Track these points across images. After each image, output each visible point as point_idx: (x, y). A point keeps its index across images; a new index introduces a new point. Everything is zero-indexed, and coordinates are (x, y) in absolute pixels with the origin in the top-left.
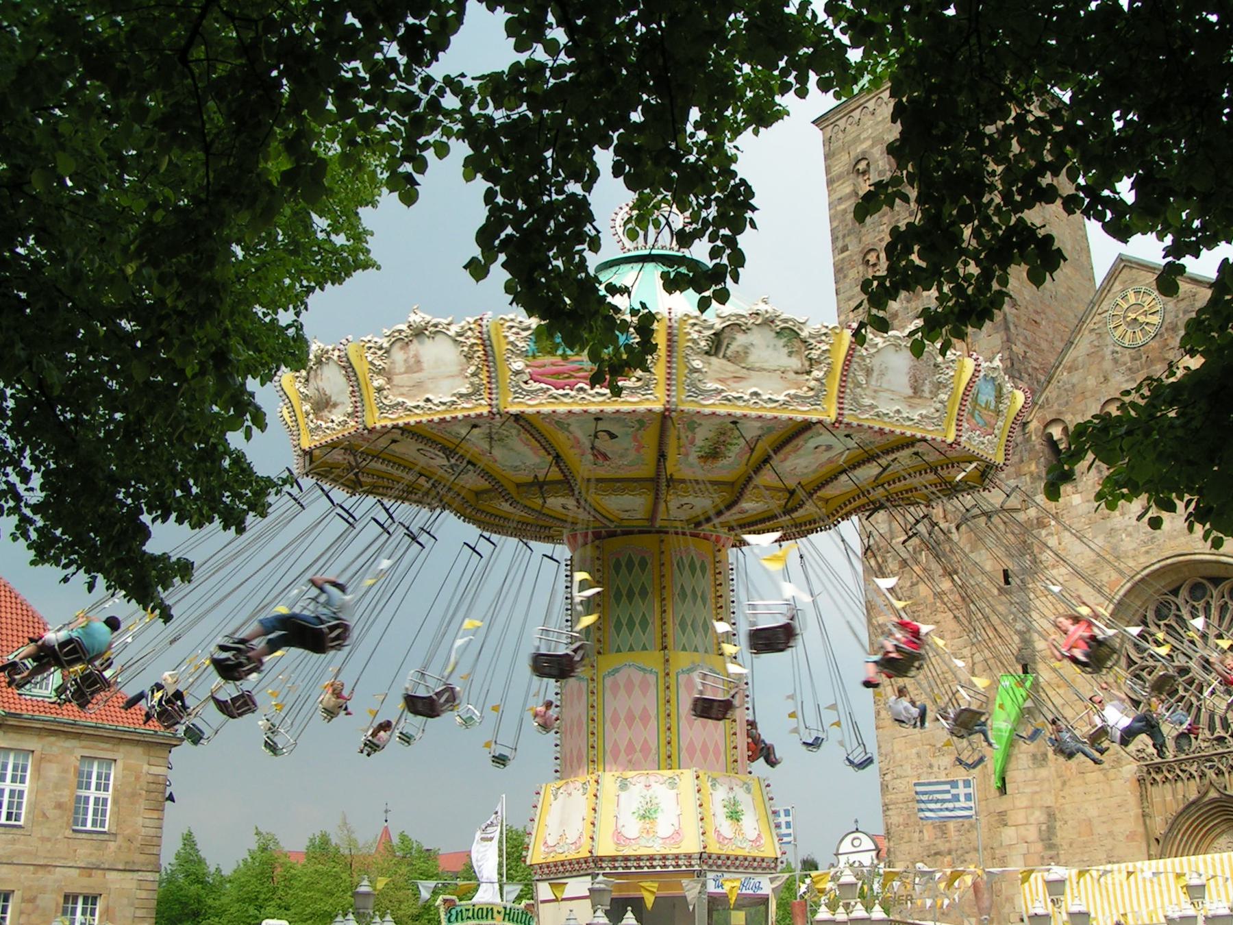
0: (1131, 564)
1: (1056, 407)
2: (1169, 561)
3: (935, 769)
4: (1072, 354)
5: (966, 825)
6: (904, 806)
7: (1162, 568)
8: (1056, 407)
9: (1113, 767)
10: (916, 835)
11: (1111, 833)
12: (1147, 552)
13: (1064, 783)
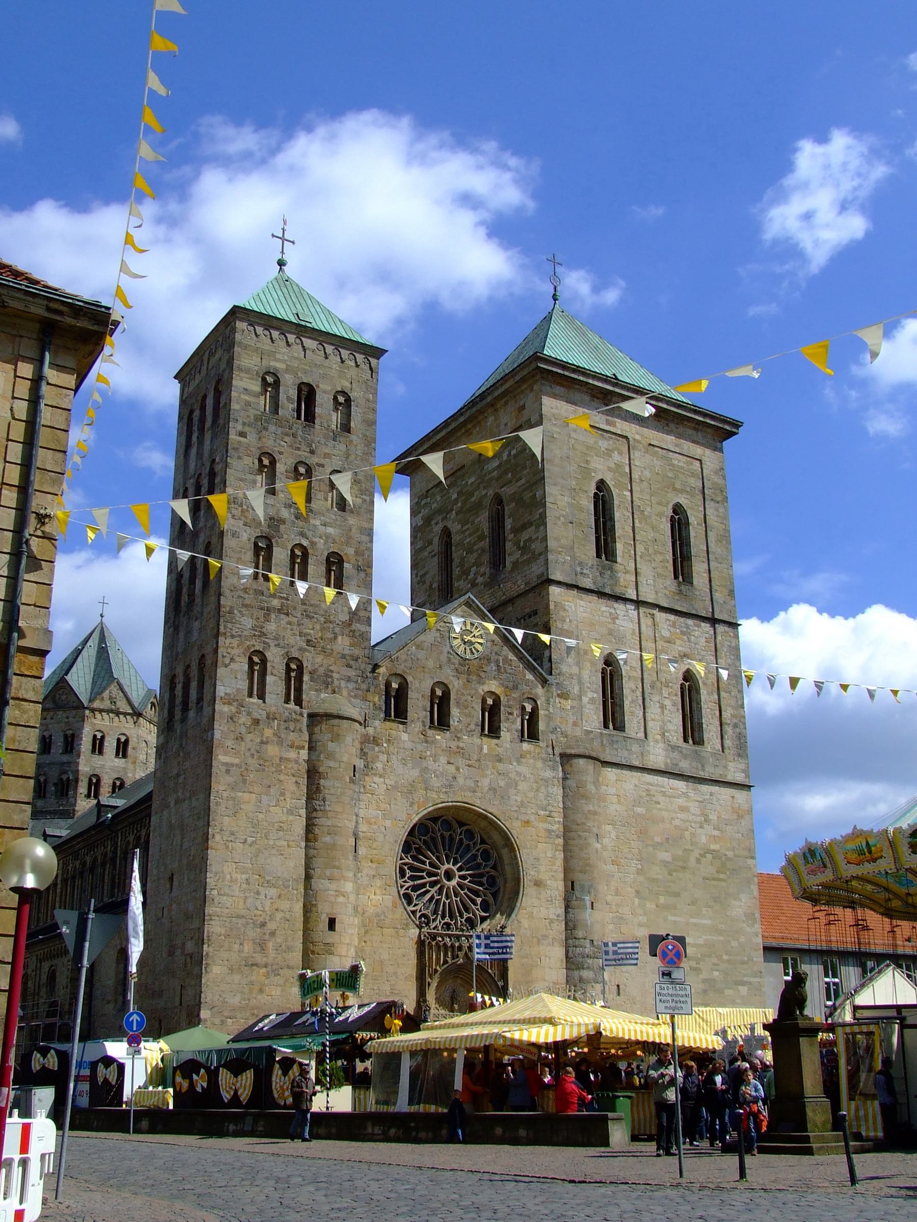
0: (435, 796)
3: (262, 897)
4: (422, 638)
5: (283, 946)
7: (460, 806)
8: (403, 666)
10: (237, 946)
11: (395, 973)
12: (446, 793)
13: (366, 932)
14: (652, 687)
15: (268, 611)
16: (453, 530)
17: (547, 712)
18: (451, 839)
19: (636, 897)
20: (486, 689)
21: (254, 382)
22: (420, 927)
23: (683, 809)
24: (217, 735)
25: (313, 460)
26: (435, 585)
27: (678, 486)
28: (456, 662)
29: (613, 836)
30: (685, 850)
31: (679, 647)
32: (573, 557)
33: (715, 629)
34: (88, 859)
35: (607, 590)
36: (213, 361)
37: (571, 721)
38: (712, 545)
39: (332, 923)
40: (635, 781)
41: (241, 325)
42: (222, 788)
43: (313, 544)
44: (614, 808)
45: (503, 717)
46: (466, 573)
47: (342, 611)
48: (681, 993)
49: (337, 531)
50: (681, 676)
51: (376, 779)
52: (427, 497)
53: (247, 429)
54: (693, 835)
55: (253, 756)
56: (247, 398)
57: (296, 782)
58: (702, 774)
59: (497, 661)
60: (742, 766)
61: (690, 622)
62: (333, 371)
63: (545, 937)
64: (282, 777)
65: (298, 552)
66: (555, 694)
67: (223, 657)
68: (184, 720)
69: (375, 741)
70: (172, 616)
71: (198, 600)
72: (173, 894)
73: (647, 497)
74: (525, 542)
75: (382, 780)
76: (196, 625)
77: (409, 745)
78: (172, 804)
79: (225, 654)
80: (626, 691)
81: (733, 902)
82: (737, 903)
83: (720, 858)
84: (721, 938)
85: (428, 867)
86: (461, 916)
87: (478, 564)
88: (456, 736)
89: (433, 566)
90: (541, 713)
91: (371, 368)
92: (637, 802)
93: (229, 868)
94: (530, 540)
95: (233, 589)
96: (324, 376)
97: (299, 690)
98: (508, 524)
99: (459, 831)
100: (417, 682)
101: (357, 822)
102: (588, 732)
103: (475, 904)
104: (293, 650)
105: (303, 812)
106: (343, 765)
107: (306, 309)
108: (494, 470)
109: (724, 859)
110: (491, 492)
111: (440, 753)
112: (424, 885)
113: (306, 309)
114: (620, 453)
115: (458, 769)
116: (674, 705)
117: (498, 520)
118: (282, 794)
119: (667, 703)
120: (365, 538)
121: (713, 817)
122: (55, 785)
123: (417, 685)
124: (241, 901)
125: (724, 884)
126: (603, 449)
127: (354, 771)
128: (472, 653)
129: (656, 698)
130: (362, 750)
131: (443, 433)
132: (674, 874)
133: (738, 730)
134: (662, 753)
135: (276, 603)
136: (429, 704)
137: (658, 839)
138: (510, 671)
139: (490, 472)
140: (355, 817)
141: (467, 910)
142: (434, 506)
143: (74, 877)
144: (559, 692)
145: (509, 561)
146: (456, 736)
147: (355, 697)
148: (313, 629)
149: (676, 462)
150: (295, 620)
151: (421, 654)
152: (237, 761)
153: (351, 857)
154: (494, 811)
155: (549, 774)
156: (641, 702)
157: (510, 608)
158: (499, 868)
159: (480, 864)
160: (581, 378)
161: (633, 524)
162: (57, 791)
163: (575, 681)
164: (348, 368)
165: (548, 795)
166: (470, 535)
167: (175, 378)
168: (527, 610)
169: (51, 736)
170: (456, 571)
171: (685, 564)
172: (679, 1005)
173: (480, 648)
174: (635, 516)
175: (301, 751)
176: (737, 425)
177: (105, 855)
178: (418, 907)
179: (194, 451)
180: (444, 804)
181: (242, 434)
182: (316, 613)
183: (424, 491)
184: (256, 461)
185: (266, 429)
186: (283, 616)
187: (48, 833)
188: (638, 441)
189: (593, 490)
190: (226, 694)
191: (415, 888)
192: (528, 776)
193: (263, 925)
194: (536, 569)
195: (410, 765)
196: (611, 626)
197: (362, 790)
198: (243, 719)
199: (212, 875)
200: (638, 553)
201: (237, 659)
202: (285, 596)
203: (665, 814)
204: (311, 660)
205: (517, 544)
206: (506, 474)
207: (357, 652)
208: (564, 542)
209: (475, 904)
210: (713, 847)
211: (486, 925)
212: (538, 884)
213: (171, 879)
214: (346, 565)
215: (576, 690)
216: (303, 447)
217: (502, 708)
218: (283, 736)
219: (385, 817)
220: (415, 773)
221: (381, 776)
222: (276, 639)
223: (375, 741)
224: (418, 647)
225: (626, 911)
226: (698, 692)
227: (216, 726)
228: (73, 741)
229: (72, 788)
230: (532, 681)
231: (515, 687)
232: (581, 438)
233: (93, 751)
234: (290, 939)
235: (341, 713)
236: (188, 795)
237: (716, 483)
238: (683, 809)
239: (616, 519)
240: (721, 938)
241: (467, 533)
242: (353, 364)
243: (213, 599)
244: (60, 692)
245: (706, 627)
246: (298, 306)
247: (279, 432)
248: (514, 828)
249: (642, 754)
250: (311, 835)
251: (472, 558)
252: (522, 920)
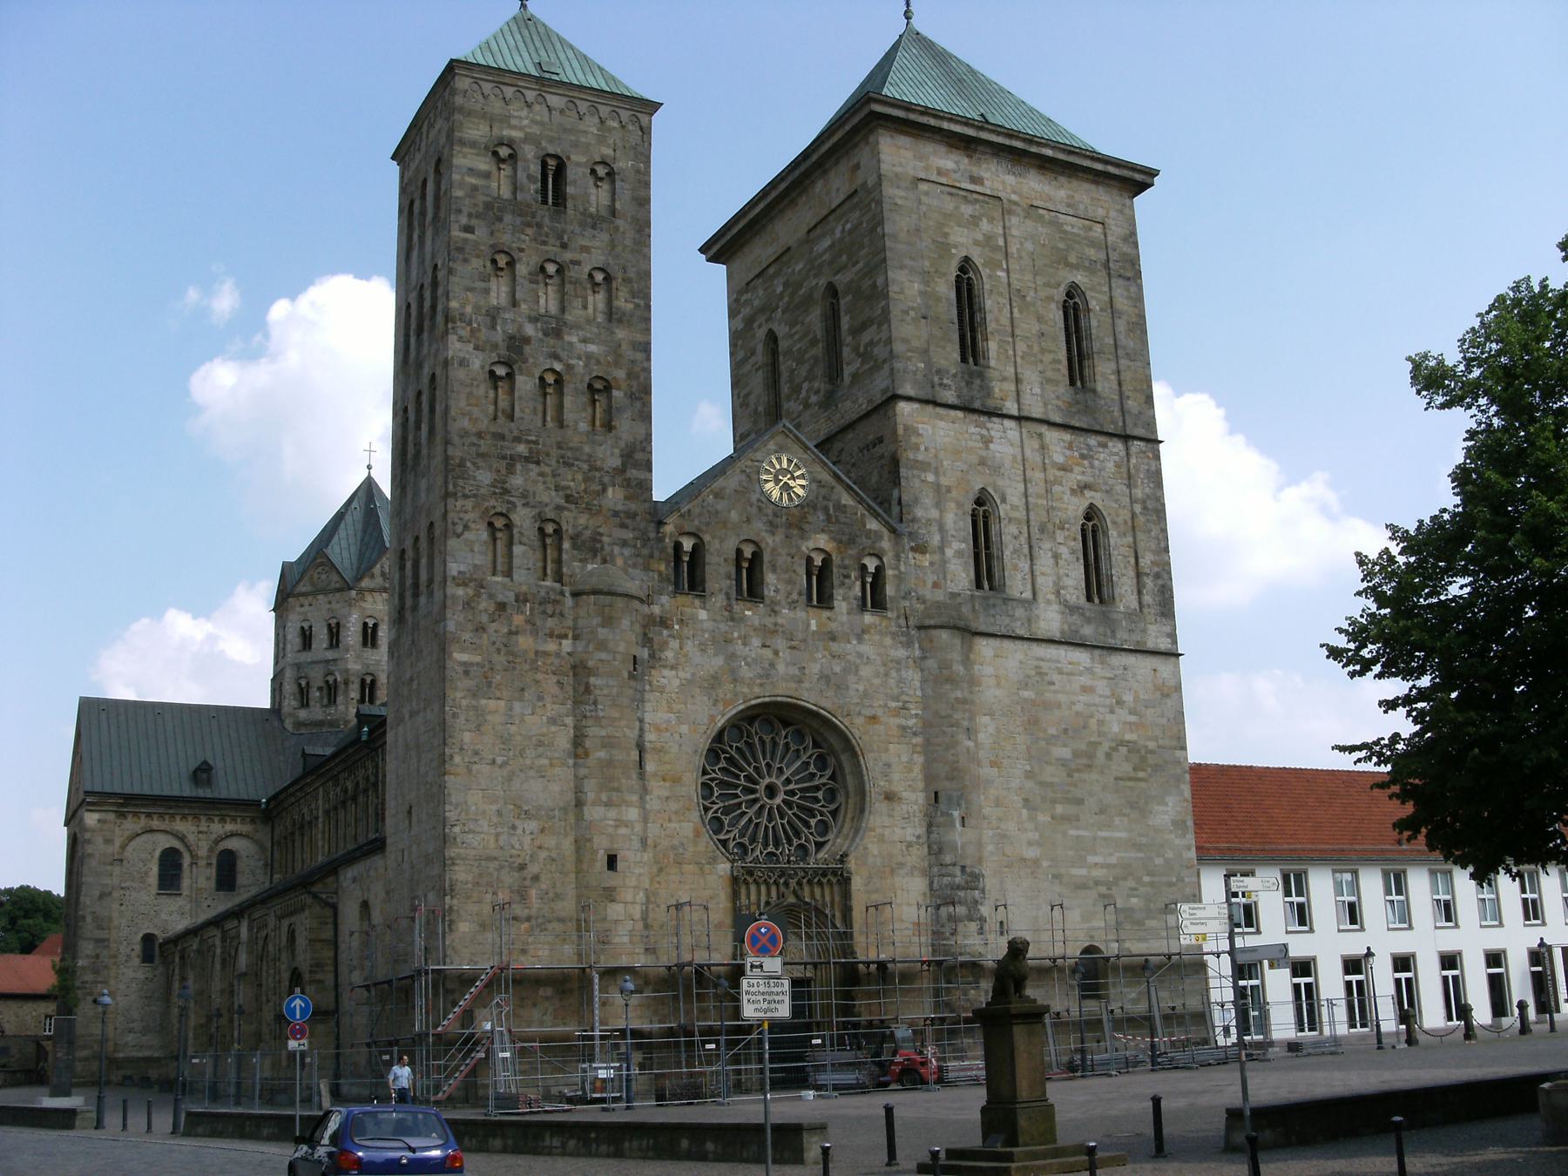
0: (746, 690)
1: (696, 522)
2: (779, 699)
3: (519, 831)
4: (719, 483)
6: (476, 864)
8: (696, 522)
9: (708, 863)
10: (489, 896)
12: (761, 685)
13: (661, 870)
14: (1042, 530)
15: (512, 461)
16: (780, 335)
17: (896, 572)
18: (775, 744)
19: (1024, 807)
20: (811, 545)
21: (483, 159)
22: (733, 861)
23: (1086, 690)
24: (451, 626)
25: (568, 256)
26: (761, 409)
27: (1072, 259)
28: (770, 512)
29: (991, 729)
30: (1090, 742)
31: (1077, 476)
32: (929, 364)
33: (1127, 449)
34: (350, 785)
35: (977, 405)
36: (433, 133)
37: (929, 583)
38: (1121, 337)
39: (612, 862)
40: (1020, 656)
41: (462, 83)
42: (459, 695)
43: (569, 367)
44: (991, 693)
45: (836, 582)
46: (797, 390)
47: (612, 454)
48: (775, 990)
49: (602, 348)
50: (1081, 512)
51: (666, 672)
52: (747, 292)
53: (474, 222)
54: (1101, 723)
55: (499, 651)
56: (473, 181)
57: (558, 682)
58: (1112, 642)
59: (826, 509)
60: (1167, 629)
61: (1093, 441)
62: (590, 136)
63: (901, 865)
64: (540, 676)
65: (550, 379)
66: (907, 547)
67: (454, 524)
68: (415, 608)
69: (664, 622)
70: (399, 471)
71: (424, 452)
72: (413, 833)
73: (1028, 277)
74: (866, 346)
75: (674, 672)
76: (423, 484)
77: (709, 625)
78: (407, 716)
79: (456, 520)
80: (1006, 538)
81: (1156, 808)
82: (1161, 808)
83: (1138, 751)
84: (1141, 855)
85: (743, 782)
86: (790, 842)
87: (810, 378)
88: (773, 611)
89: (757, 382)
90: (889, 572)
91: (641, 129)
92: (1024, 685)
93: (474, 799)
94: (871, 344)
95: (464, 434)
96: (575, 145)
97: (559, 562)
98: (845, 322)
99: (784, 733)
100: (717, 541)
101: (641, 729)
102: (954, 595)
103: (809, 827)
104: (547, 510)
105: (569, 721)
106: (619, 657)
107: (552, 56)
108: (824, 252)
109: (1143, 752)
110: (823, 282)
111: (752, 633)
112: (740, 804)
113: (552, 56)
114: (991, 220)
115: (776, 653)
116: (1073, 552)
117: (833, 317)
118: (540, 698)
119: (1064, 551)
120: (639, 356)
121: (1128, 698)
122: (320, 689)
123: (718, 546)
124: (492, 839)
125: (1143, 785)
126: (966, 216)
127: (635, 663)
128: (791, 499)
129: (1047, 545)
130: (645, 634)
131: (762, 206)
132: (1076, 775)
133: (1160, 582)
134: (1058, 617)
135: (522, 449)
136: (733, 570)
137: (1052, 731)
138: (843, 520)
139: (821, 255)
140: (637, 723)
141: (798, 834)
142: (756, 303)
143: (336, 808)
144: (913, 544)
145: (847, 372)
146: (773, 611)
147: (635, 566)
148: (573, 480)
149: (1069, 228)
150: (547, 470)
151: (721, 505)
152: (478, 659)
153: (634, 776)
154: (828, 705)
155: (901, 653)
156: (1026, 550)
157: (850, 436)
158: (839, 778)
159: (813, 775)
160: (932, 122)
161: (1012, 313)
162: (321, 698)
163: (934, 528)
164: (610, 130)
165: (901, 681)
166: (800, 340)
167: (393, 158)
168: (871, 437)
169: (311, 627)
170: (785, 389)
171: (1086, 363)
172: (773, 1006)
173: (800, 492)
174: (1014, 304)
175: (564, 642)
176: (1153, 173)
177: (367, 779)
178: (732, 835)
179: (415, 253)
180: (759, 701)
181: (469, 229)
182: (577, 459)
183: (743, 284)
184: (488, 264)
185: (500, 219)
186: (532, 466)
187: (307, 752)
188: (1016, 203)
189: (953, 272)
190: (460, 572)
191: (727, 811)
192: (872, 657)
193: (522, 867)
194: (880, 383)
195: (710, 651)
196: (984, 453)
197: (647, 687)
198: (484, 604)
199: (452, 808)
200: (1019, 353)
201: (473, 526)
202: (534, 438)
203: (1062, 698)
204: (574, 521)
205: (856, 349)
206: (841, 256)
207: (633, 506)
208: (915, 343)
209: (809, 827)
210: (1128, 737)
211: (821, 855)
212: (890, 797)
213: (410, 812)
214: (615, 393)
215: (936, 539)
216: (552, 240)
217: (835, 570)
218: (539, 623)
219: (680, 721)
220: (719, 661)
221: (672, 668)
222: (524, 495)
223: (664, 622)
224: (717, 496)
225: (1011, 827)
226: (1106, 534)
227: (449, 615)
228: (338, 632)
229: (340, 692)
230: (875, 532)
231: (852, 541)
232: (935, 202)
233: (365, 644)
234: (558, 884)
235: (614, 589)
236: (422, 705)
237: (1125, 254)
238: (1086, 690)
239: (987, 307)
240: (1141, 855)
241: (797, 337)
242: (615, 124)
243: (439, 449)
244: (320, 570)
245: (1117, 446)
246: (543, 53)
247: (518, 223)
248: (856, 727)
249: (1029, 620)
250: (580, 751)
251: (803, 371)
252: (870, 846)
